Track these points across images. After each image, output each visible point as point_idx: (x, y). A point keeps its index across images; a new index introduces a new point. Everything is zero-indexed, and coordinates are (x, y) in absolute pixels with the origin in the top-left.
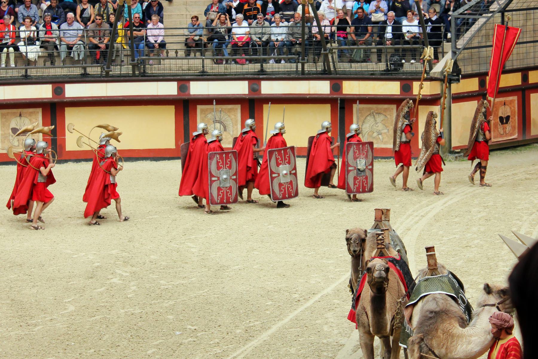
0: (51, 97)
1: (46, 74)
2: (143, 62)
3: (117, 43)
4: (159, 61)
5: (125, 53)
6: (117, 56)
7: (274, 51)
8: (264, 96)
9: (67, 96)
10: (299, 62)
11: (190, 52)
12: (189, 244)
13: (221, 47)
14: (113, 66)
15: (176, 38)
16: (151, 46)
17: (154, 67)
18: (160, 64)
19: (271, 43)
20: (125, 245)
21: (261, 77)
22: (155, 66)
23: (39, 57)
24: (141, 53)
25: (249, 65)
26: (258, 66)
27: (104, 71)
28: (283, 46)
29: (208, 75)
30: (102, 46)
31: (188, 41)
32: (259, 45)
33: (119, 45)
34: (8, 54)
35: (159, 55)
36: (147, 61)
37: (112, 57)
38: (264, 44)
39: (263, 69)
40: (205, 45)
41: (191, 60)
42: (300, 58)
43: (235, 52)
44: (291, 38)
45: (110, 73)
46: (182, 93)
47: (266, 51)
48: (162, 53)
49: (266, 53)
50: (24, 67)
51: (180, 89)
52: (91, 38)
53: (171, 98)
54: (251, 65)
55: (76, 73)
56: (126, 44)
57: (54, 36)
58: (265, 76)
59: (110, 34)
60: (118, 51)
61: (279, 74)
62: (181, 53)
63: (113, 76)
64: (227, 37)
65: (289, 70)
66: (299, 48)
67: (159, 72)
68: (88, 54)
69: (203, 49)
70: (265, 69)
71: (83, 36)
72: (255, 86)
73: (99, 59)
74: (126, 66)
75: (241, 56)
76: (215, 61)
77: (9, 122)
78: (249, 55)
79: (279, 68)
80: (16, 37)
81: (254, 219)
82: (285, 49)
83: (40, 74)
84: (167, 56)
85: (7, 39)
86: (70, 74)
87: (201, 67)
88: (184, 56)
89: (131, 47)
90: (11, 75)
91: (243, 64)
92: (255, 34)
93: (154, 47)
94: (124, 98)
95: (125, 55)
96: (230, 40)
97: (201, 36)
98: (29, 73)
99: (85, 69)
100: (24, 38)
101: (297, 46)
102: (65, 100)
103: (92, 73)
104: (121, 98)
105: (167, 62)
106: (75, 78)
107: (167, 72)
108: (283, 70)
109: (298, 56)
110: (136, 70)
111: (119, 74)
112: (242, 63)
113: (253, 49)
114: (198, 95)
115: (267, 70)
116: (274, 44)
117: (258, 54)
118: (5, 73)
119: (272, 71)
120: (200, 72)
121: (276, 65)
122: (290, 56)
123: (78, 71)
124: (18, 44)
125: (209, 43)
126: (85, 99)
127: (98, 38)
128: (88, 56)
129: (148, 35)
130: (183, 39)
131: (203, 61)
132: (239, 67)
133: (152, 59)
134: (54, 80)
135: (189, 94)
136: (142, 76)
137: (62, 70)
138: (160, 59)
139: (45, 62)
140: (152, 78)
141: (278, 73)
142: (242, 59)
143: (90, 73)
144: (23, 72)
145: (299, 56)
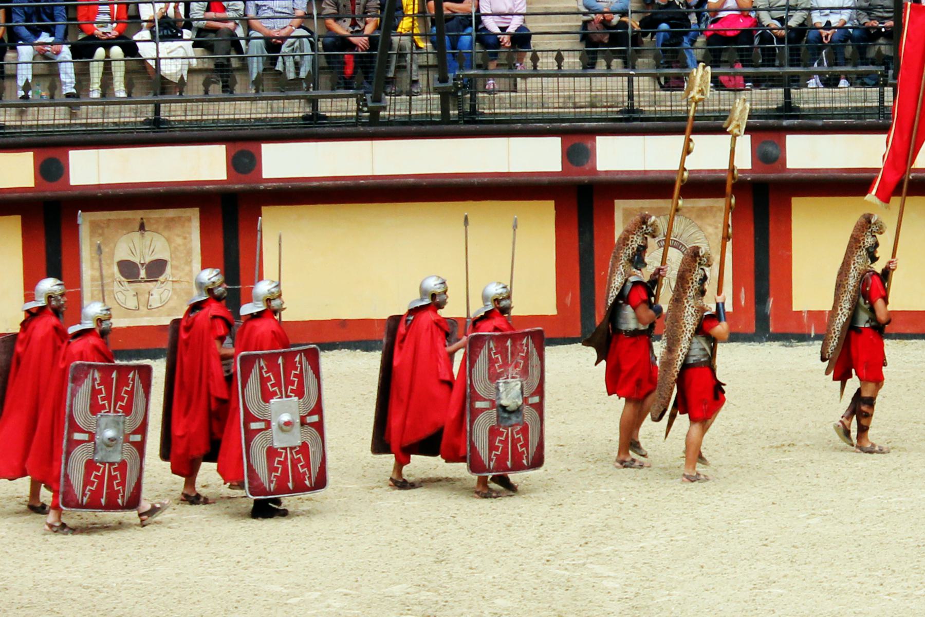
0: (224, 177)
1: (210, 117)
2: (471, 85)
3: (401, 34)
4: (512, 80)
5: (422, 60)
6: (400, 68)
7: (820, 54)
8: (793, 175)
9: (266, 175)
10: (886, 84)
11: (596, 58)
12: (598, 569)
13: (679, 43)
14: (390, 94)
15: (556, 21)
16: (491, 40)
17: (500, 98)
18: (516, 91)
19: (811, 34)
20: (427, 571)
21: (785, 123)
22: (502, 94)
23: (191, 71)
24: (463, 61)
25: (754, 91)
26: (776, 95)
27: (365, 109)
28: (845, 40)
29: (642, 120)
30: (360, 41)
31: (591, 29)
32: (781, 40)
33: (406, 40)
34: (107, 64)
35: (512, 66)
36: (480, 82)
37: (387, 72)
38: (793, 35)
39: (790, 103)
40: (636, 39)
41: (599, 79)
42: (891, 72)
43: (715, 56)
44: (865, 20)
45: (382, 113)
46: (574, 168)
47: (799, 55)
48: (521, 60)
49: (799, 60)
50: (150, 97)
51: (571, 155)
52: (330, 22)
53: (545, 179)
54: (758, 91)
55: (291, 115)
56: (425, 36)
57: (230, 14)
58: (796, 122)
59: (382, 9)
60: (401, 56)
61: (833, 116)
62: (572, 60)
63: (389, 123)
64: (693, 19)
65: (859, 105)
66: (887, 47)
67: (513, 111)
68: (323, 62)
69: (630, 48)
70: (795, 104)
71: (308, 16)
72: (771, 149)
73: (351, 78)
74: (424, 96)
75: (732, 67)
76: (662, 81)
77: (112, 245)
78: (752, 66)
79: (833, 100)
80: (130, 17)
81: (771, 501)
82: (849, 50)
83: (194, 118)
84: (535, 67)
85: (104, 24)
86: (274, 115)
87: (626, 99)
88: (578, 68)
89: (438, 45)
90: (116, 120)
91: (736, 90)
92: (769, 9)
93: (498, 44)
94: (419, 180)
95: (421, 67)
96: (703, 26)
97: (624, 13)
98: (164, 115)
99: (313, 102)
100: (151, 21)
101: (881, 41)
102: (262, 187)
103: (334, 114)
104: (412, 180)
105: (534, 85)
106: (288, 127)
107: (535, 111)
108: (843, 105)
109: (883, 68)
110: (451, 106)
111: (405, 116)
112: (734, 86)
113: (763, 50)
114: (618, 172)
115: (802, 106)
116: (820, 34)
117: (777, 63)
118: (99, 116)
119: (815, 109)
120: (618, 112)
121: (825, 92)
122: (862, 68)
123: (296, 110)
124: (136, 38)
125: (645, 34)
126: (315, 184)
127: (349, 21)
128: (323, 68)
129: (482, 12)
130: (576, 22)
131: (630, 82)
132: (727, 97)
133: (494, 76)
134: (231, 133)
135: (594, 170)
136: (466, 122)
137: (254, 106)
138: (515, 77)
139: (206, 84)
140: (495, 126)
141: (831, 113)
142: (736, 74)
143: (328, 114)
144: (148, 112)
145: (887, 69)
